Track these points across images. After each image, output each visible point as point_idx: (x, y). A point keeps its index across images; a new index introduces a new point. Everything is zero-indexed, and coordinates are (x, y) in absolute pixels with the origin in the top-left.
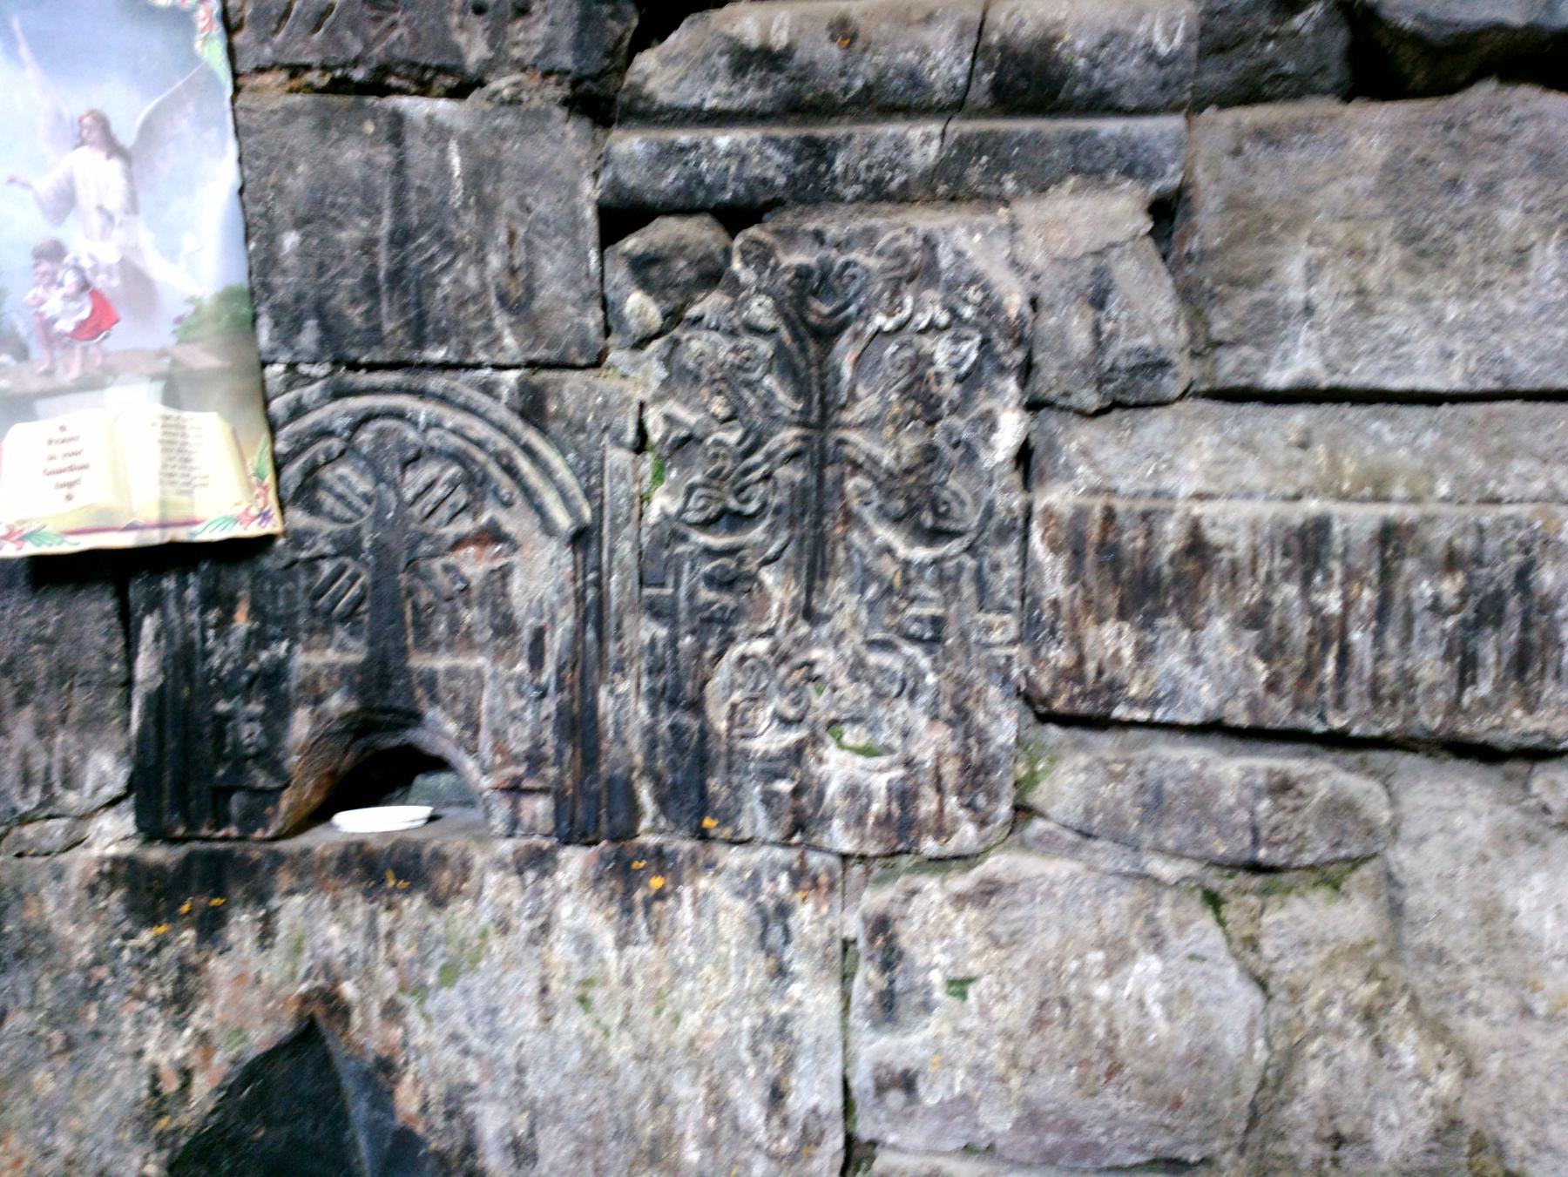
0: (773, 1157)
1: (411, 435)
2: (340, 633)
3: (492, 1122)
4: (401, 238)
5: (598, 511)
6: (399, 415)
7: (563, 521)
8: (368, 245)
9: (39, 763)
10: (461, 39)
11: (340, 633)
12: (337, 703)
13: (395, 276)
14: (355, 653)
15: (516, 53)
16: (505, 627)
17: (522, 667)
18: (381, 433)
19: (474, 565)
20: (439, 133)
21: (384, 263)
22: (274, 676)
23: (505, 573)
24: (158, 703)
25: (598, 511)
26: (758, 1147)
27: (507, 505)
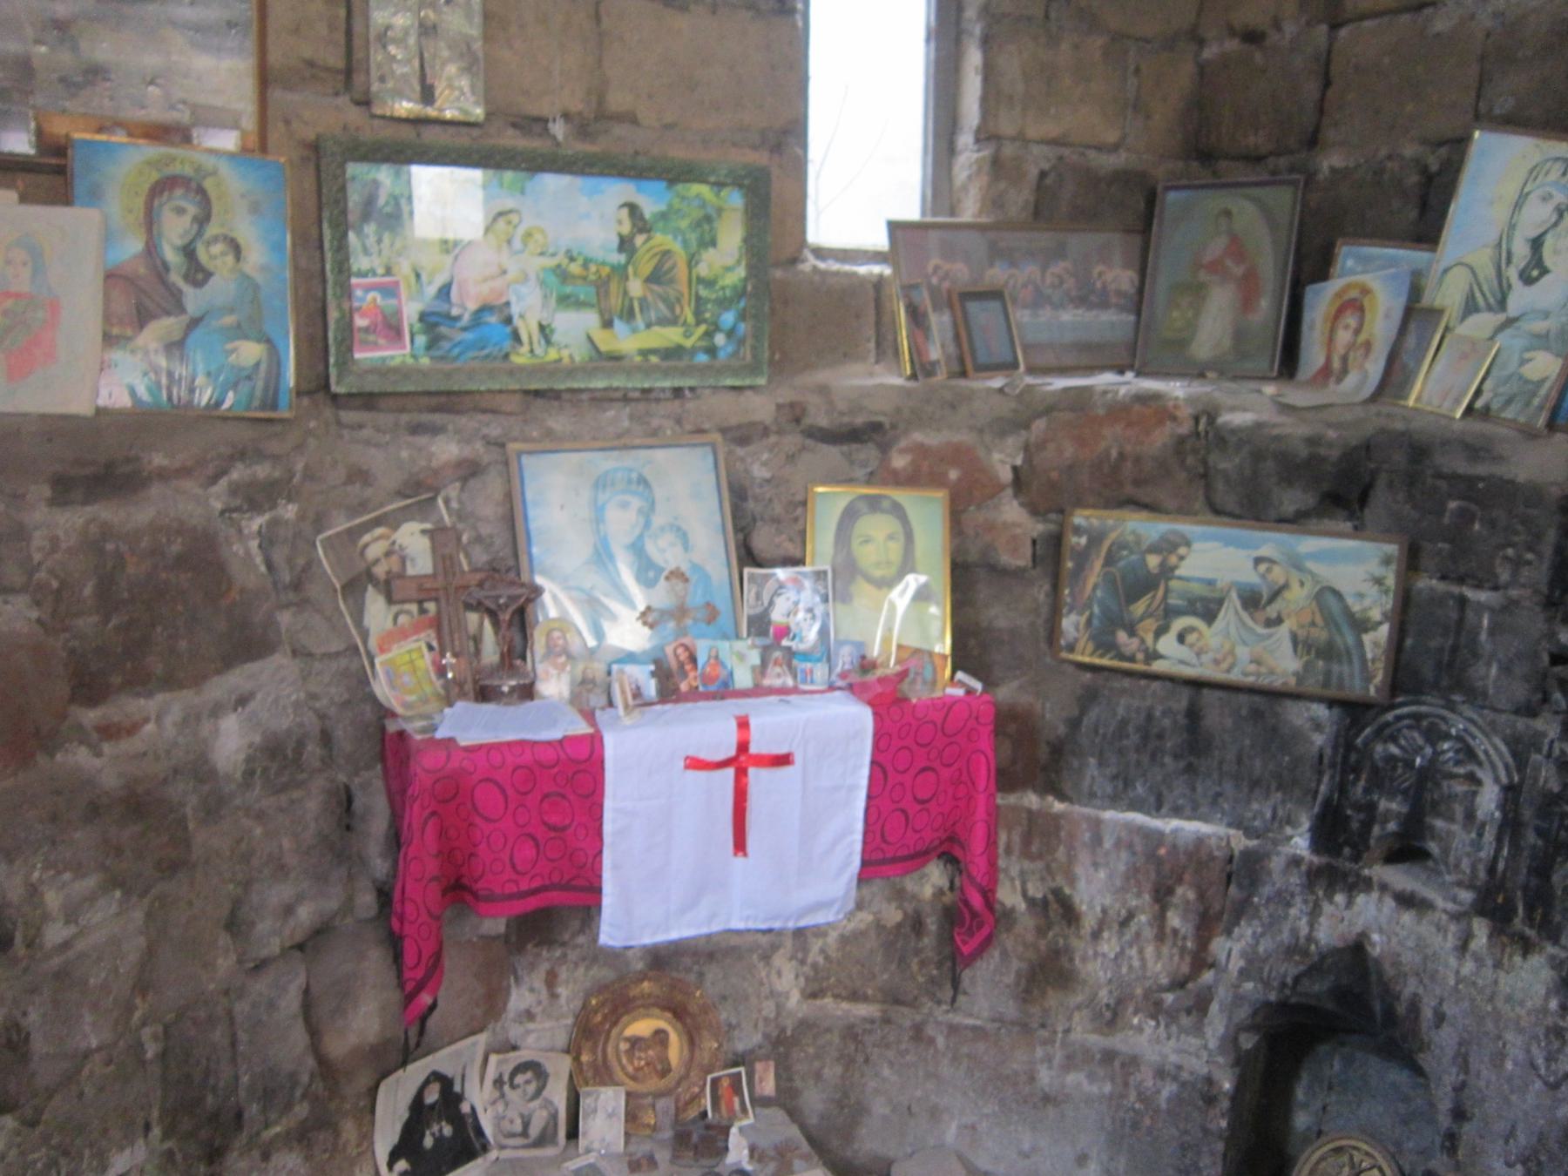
0: (1546, 1083)
1: (1444, 727)
2: (1399, 798)
3: (1427, 1013)
4: (1455, 649)
5: (1522, 781)
6: (1443, 719)
7: (1504, 780)
8: (1441, 650)
9: (1280, 813)
10: (1499, 570)
11: (1399, 798)
12: (1392, 826)
13: (1450, 665)
14: (1405, 809)
15: (1522, 580)
16: (1470, 816)
17: (1473, 835)
18: (1432, 724)
19: (1460, 788)
20: (1480, 607)
21: (1446, 658)
22: (1371, 807)
23: (1475, 793)
24: (1327, 803)
25: (1522, 781)
26: (1539, 1076)
27: (1480, 764)
